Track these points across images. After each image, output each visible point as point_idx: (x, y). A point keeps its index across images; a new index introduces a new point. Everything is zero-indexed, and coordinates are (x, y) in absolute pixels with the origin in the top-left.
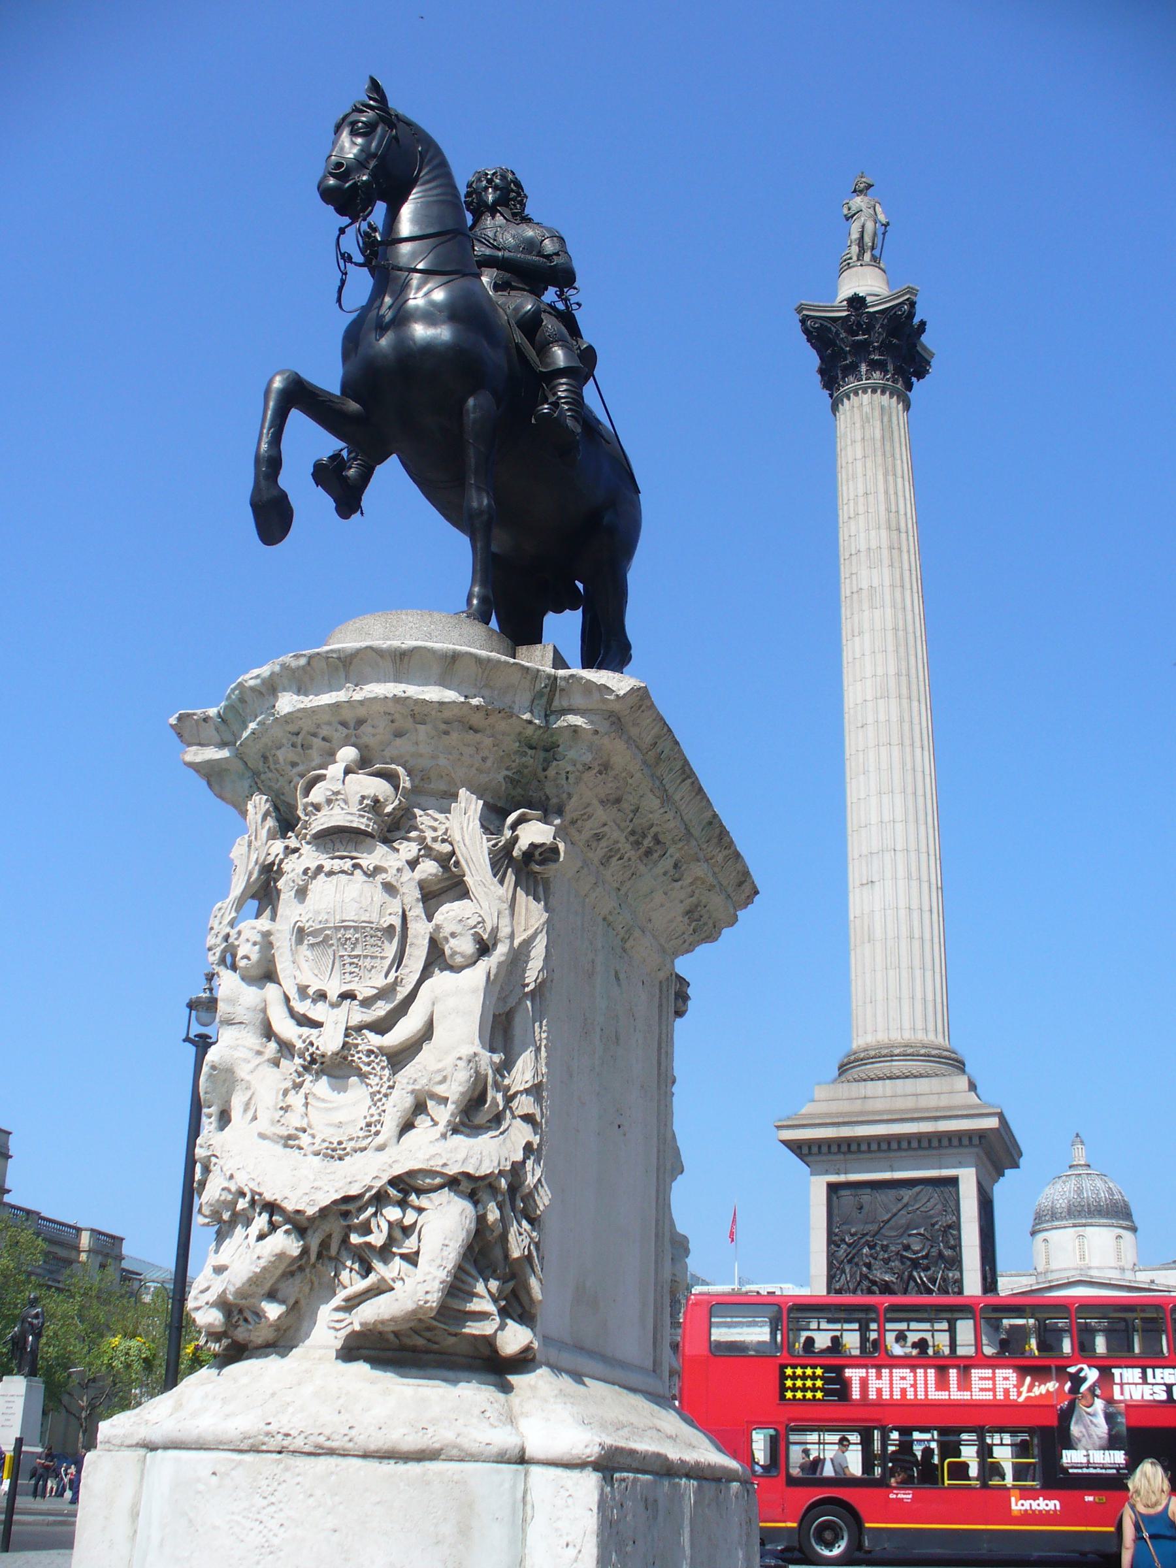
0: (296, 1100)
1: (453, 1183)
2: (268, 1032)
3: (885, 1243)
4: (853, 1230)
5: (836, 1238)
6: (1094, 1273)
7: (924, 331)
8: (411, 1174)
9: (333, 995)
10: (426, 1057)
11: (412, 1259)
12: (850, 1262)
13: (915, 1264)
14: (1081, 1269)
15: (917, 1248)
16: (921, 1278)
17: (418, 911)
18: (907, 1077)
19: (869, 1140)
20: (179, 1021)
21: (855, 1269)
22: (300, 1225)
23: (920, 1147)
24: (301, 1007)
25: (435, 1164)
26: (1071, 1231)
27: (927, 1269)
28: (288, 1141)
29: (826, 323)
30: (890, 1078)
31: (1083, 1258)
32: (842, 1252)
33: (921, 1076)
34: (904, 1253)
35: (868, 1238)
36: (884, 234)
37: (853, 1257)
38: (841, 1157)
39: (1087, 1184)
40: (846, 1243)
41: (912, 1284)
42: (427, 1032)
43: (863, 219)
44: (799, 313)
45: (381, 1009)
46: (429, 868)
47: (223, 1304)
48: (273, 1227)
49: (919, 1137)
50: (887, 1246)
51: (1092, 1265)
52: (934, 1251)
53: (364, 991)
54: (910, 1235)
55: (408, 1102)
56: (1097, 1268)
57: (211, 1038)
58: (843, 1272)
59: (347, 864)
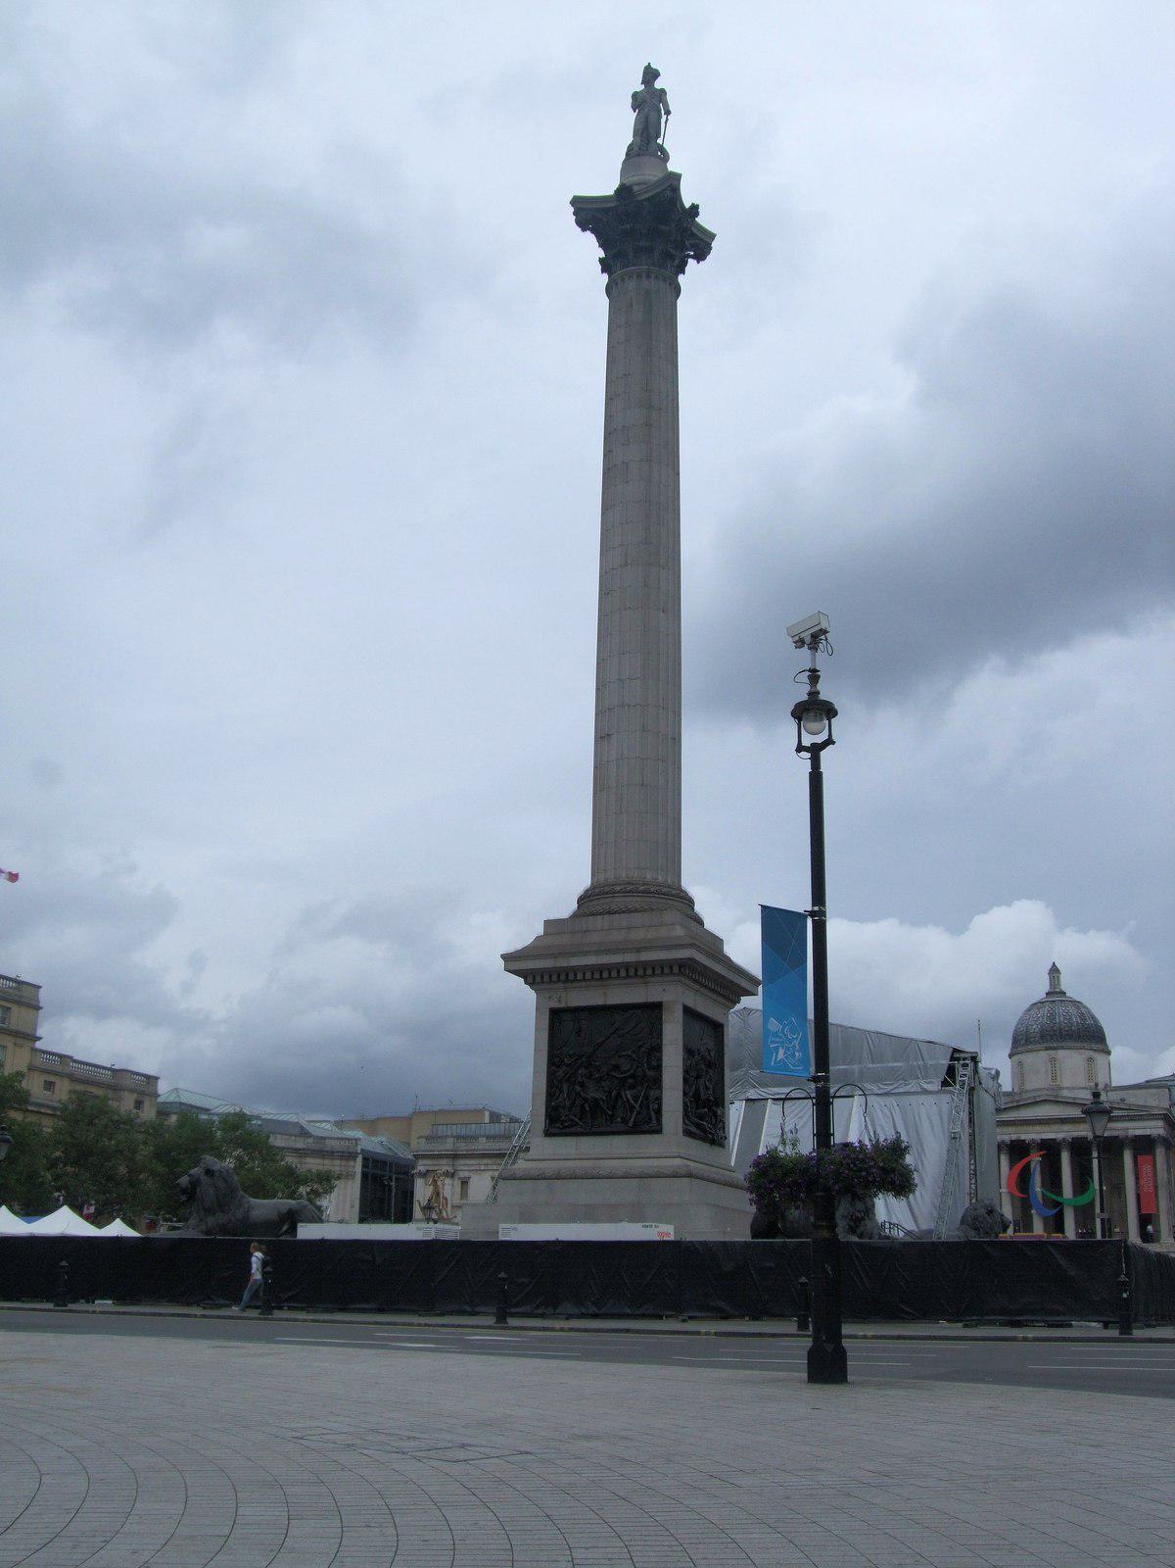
5: (556, 1060)
6: (1065, 1093)
7: (697, 214)
12: (568, 1080)
14: (1053, 1089)
18: (624, 912)
19: (584, 969)
23: (628, 976)
26: (1043, 1054)
27: (632, 1087)
30: (609, 913)
31: (1054, 1079)
32: (560, 1073)
33: (636, 911)
34: (613, 1074)
38: (560, 985)
39: (1060, 1009)
41: (620, 1102)
49: (627, 966)
51: (1065, 1085)
56: (1068, 1088)
58: (561, 1091)
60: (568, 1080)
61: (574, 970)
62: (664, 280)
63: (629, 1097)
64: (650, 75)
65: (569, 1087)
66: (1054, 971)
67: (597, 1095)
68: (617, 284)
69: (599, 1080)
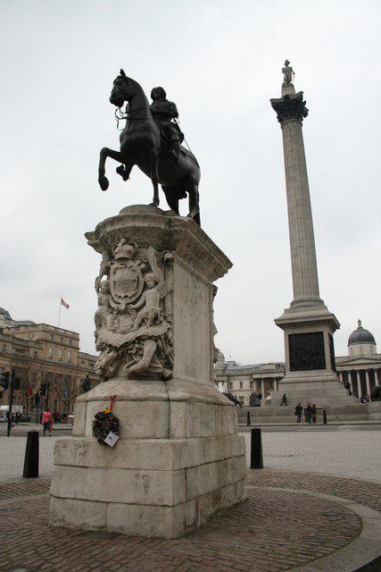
0: (116, 321)
1: (150, 338)
2: (110, 306)
10: (144, 310)
11: (142, 356)
17: (141, 276)
19: (301, 323)
22: (116, 349)
24: (116, 299)
28: (114, 331)
42: (144, 304)
46: (143, 266)
47: (101, 368)
55: (140, 320)
61: (296, 323)
64: (287, 63)
66: (359, 321)
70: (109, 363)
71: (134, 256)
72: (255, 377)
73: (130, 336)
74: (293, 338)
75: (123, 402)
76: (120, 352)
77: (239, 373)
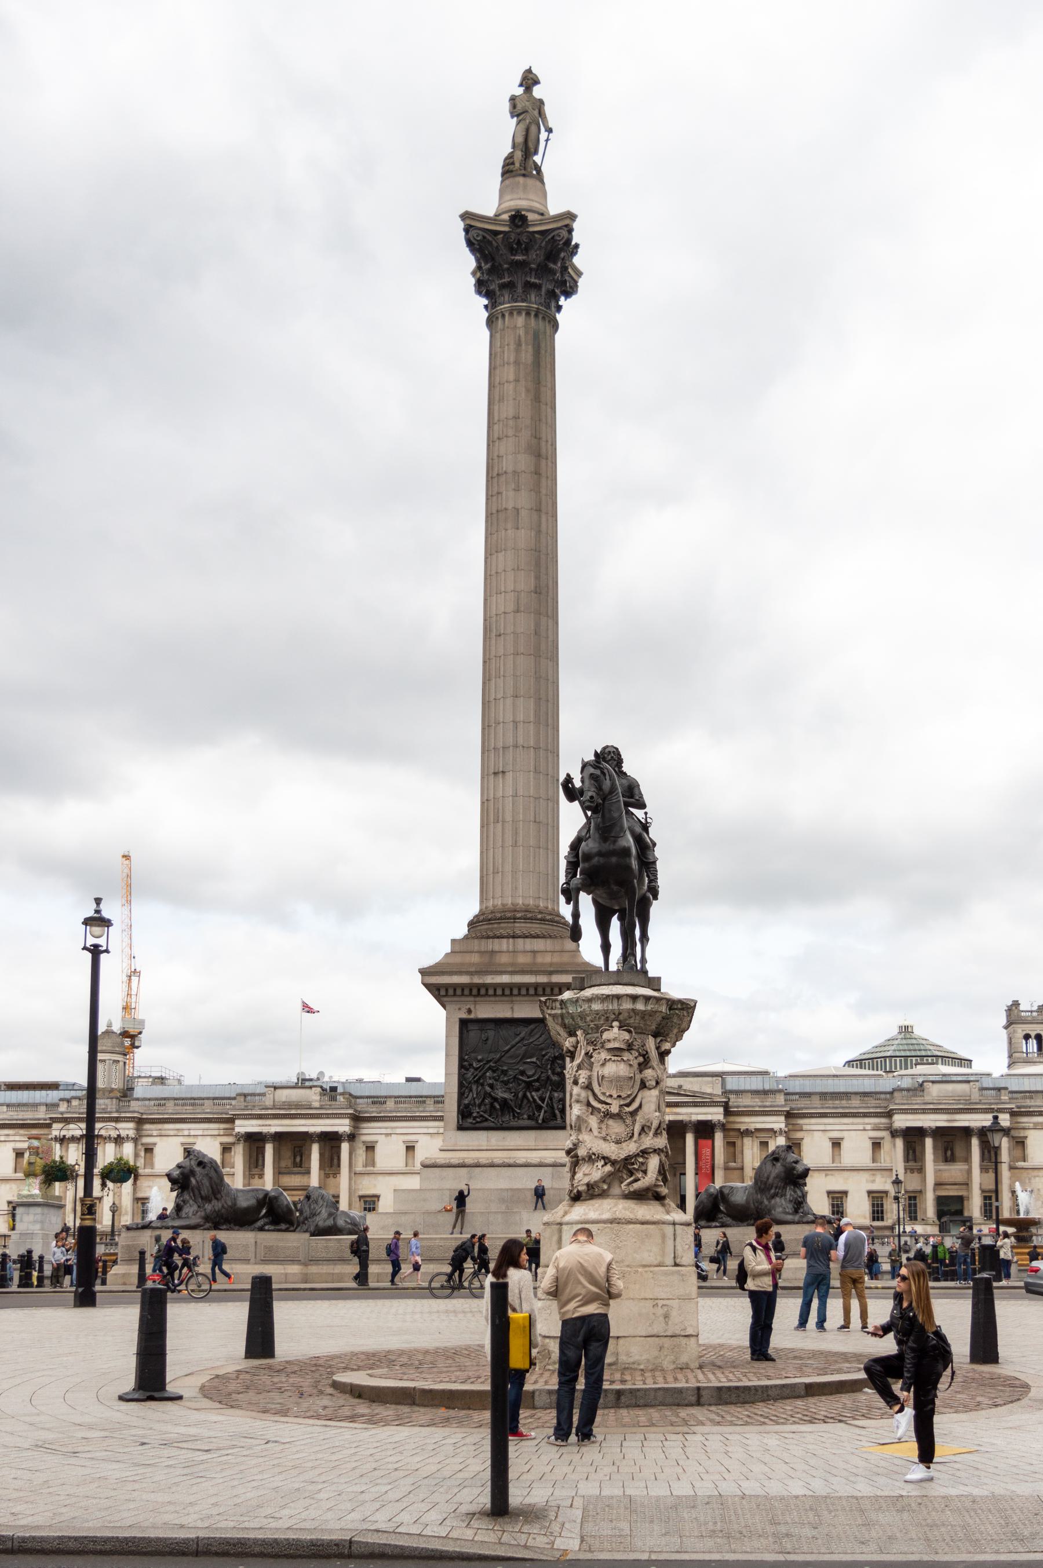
0: (604, 1126)
2: (589, 1104)
3: (505, 1068)
4: (479, 1057)
5: (466, 1063)
8: (646, 1149)
9: (607, 1094)
11: (645, 1172)
12: (477, 1082)
13: (529, 1086)
15: (530, 1073)
16: (532, 1097)
20: (78, 935)
21: (480, 1088)
22: (614, 1163)
24: (602, 1098)
25: (652, 1146)
27: (537, 1090)
28: (605, 1139)
29: (488, 237)
32: (469, 1075)
35: (492, 1064)
36: (547, 140)
37: (479, 1079)
40: (474, 1068)
41: (525, 1101)
42: (640, 1106)
43: (528, 121)
44: (463, 220)
45: (628, 1101)
46: (641, 1059)
48: (606, 1164)
50: (506, 1071)
52: (544, 1077)
53: (624, 1095)
54: (525, 1063)
57: (101, 946)
58: (471, 1090)
59: (619, 1058)
60: (477, 1082)
62: (549, 322)
63: (536, 1097)
64: (529, 80)
65: (477, 1087)
67: (506, 1095)
68: (503, 316)
69: (506, 1083)
70: (603, 1180)
71: (630, 1047)
72: (244, 1126)
73: (631, 1148)
74: (474, 1034)
75: (631, 1226)
76: (618, 1167)
77: (187, 1112)
